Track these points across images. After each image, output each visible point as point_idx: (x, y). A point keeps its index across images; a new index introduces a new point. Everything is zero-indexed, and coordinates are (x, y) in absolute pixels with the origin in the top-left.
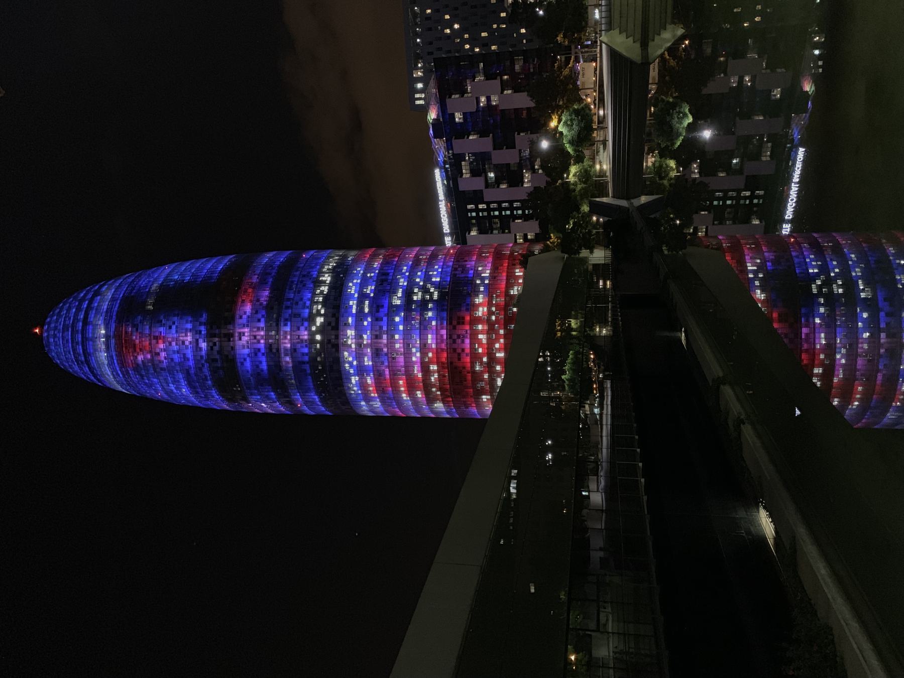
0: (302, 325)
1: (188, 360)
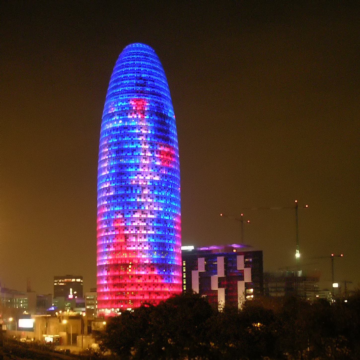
0: (151, 191)
1: (133, 130)
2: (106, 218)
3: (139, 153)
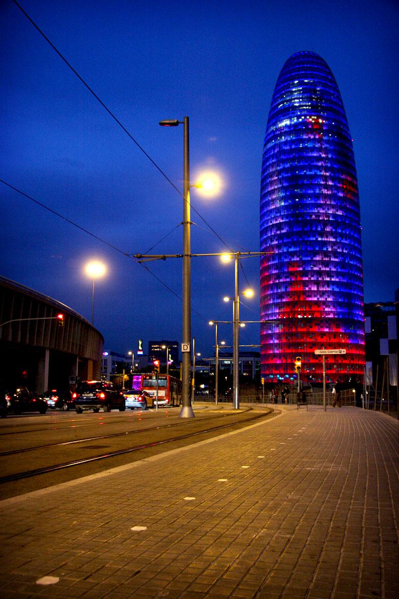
2: (276, 262)
3: (319, 181)
